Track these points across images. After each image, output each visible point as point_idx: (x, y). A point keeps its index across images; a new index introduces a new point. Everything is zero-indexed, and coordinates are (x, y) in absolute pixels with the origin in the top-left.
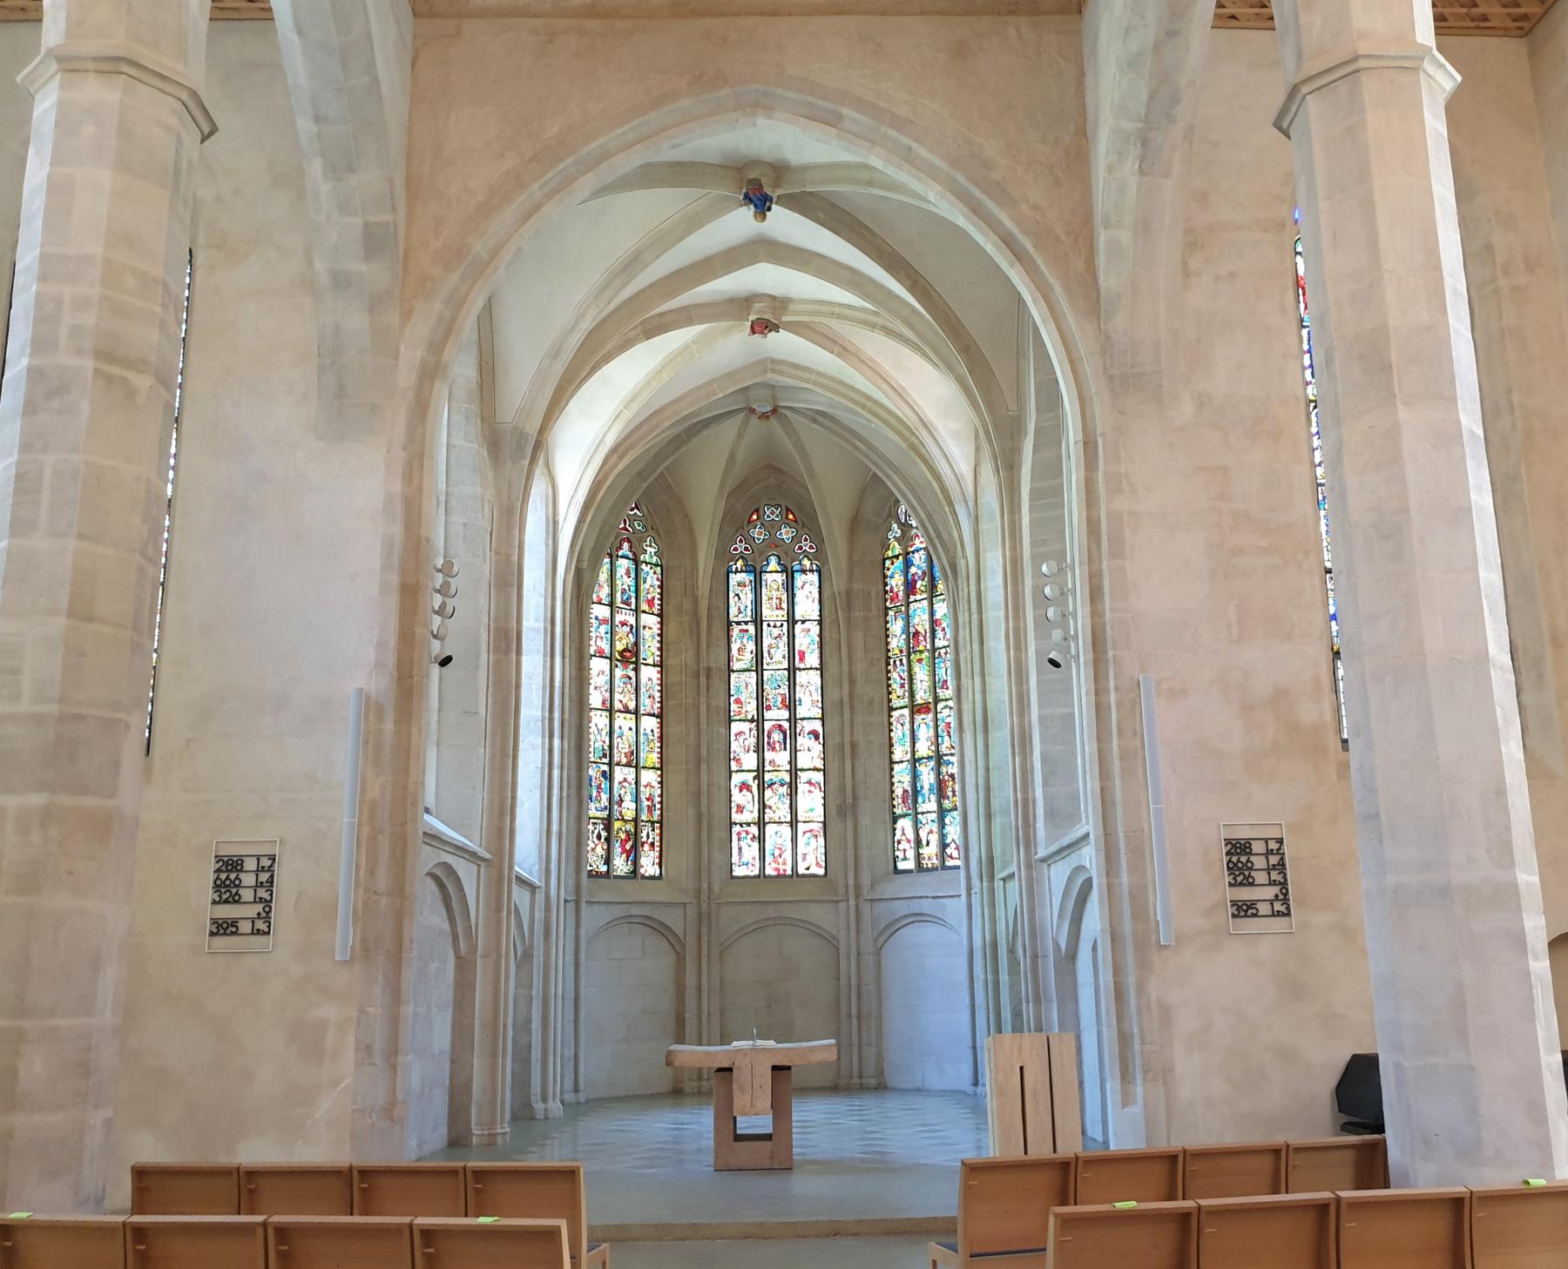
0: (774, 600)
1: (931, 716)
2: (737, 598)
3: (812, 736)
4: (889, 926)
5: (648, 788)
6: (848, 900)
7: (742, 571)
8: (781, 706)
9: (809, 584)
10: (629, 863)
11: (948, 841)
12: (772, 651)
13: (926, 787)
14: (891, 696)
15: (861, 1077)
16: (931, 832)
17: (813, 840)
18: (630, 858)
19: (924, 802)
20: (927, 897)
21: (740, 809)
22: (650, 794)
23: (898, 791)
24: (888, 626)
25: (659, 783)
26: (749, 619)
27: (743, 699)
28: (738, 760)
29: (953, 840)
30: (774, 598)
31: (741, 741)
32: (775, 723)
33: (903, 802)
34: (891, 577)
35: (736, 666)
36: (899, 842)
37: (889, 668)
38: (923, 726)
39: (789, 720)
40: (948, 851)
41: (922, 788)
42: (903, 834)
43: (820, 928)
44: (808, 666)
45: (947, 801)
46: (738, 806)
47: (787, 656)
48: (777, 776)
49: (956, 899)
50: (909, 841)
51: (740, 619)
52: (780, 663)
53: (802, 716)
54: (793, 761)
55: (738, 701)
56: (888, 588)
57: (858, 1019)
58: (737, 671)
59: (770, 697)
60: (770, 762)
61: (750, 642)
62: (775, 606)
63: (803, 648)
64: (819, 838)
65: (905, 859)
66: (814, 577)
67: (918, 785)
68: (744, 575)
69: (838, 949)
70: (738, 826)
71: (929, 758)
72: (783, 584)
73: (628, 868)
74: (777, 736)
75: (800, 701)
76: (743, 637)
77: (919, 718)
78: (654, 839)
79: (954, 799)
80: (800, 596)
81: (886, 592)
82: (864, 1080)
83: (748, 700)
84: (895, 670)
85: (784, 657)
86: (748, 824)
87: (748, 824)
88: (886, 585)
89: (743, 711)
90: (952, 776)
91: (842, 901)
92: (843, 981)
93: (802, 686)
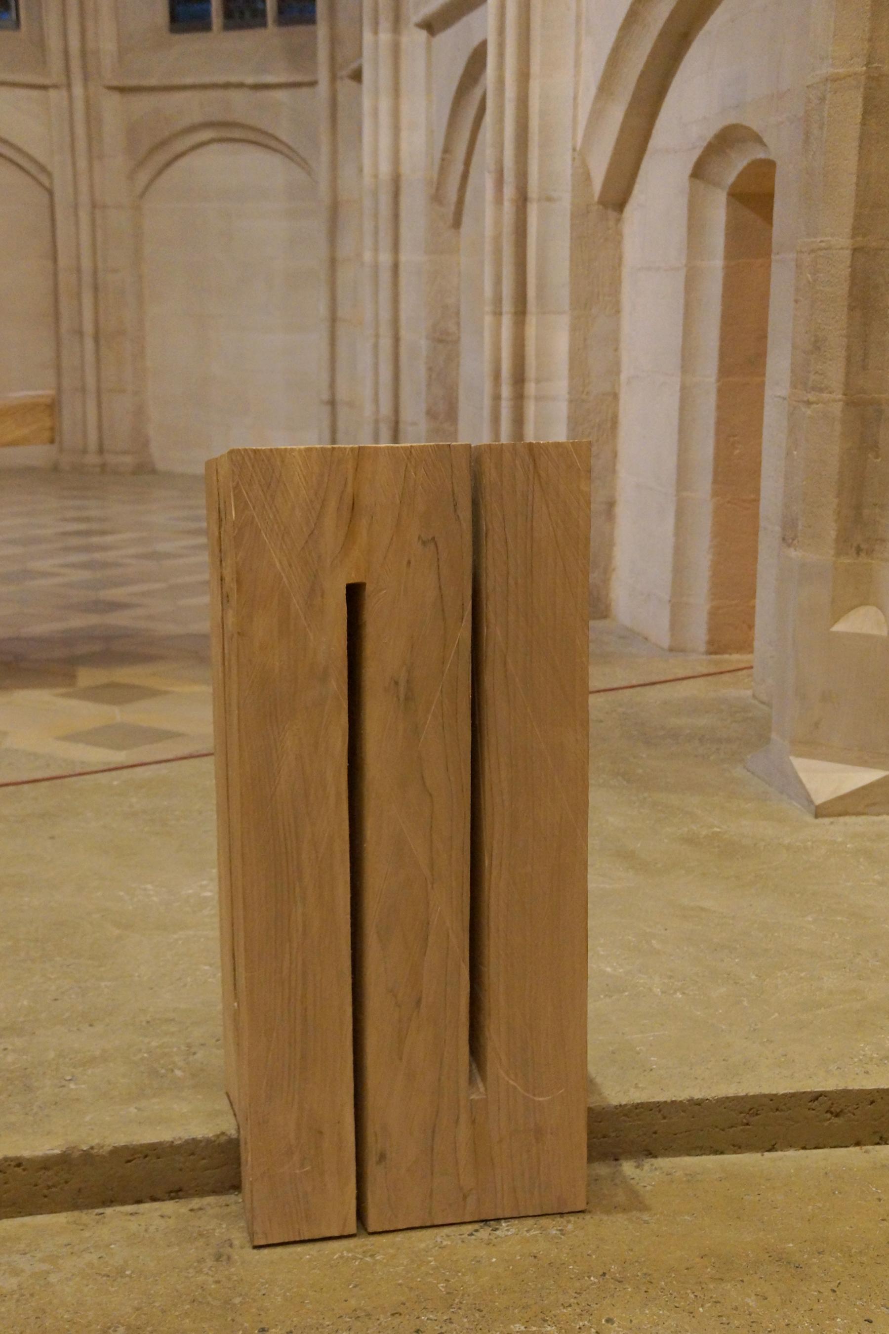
4: (164, 143)
6: (69, 86)
15: (101, 451)
20: (240, 86)
43: (19, 150)
49: (305, 91)
57: (96, 339)
69: (51, 193)
82: (111, 459)
91: (55, 86)
92: (63, 261)
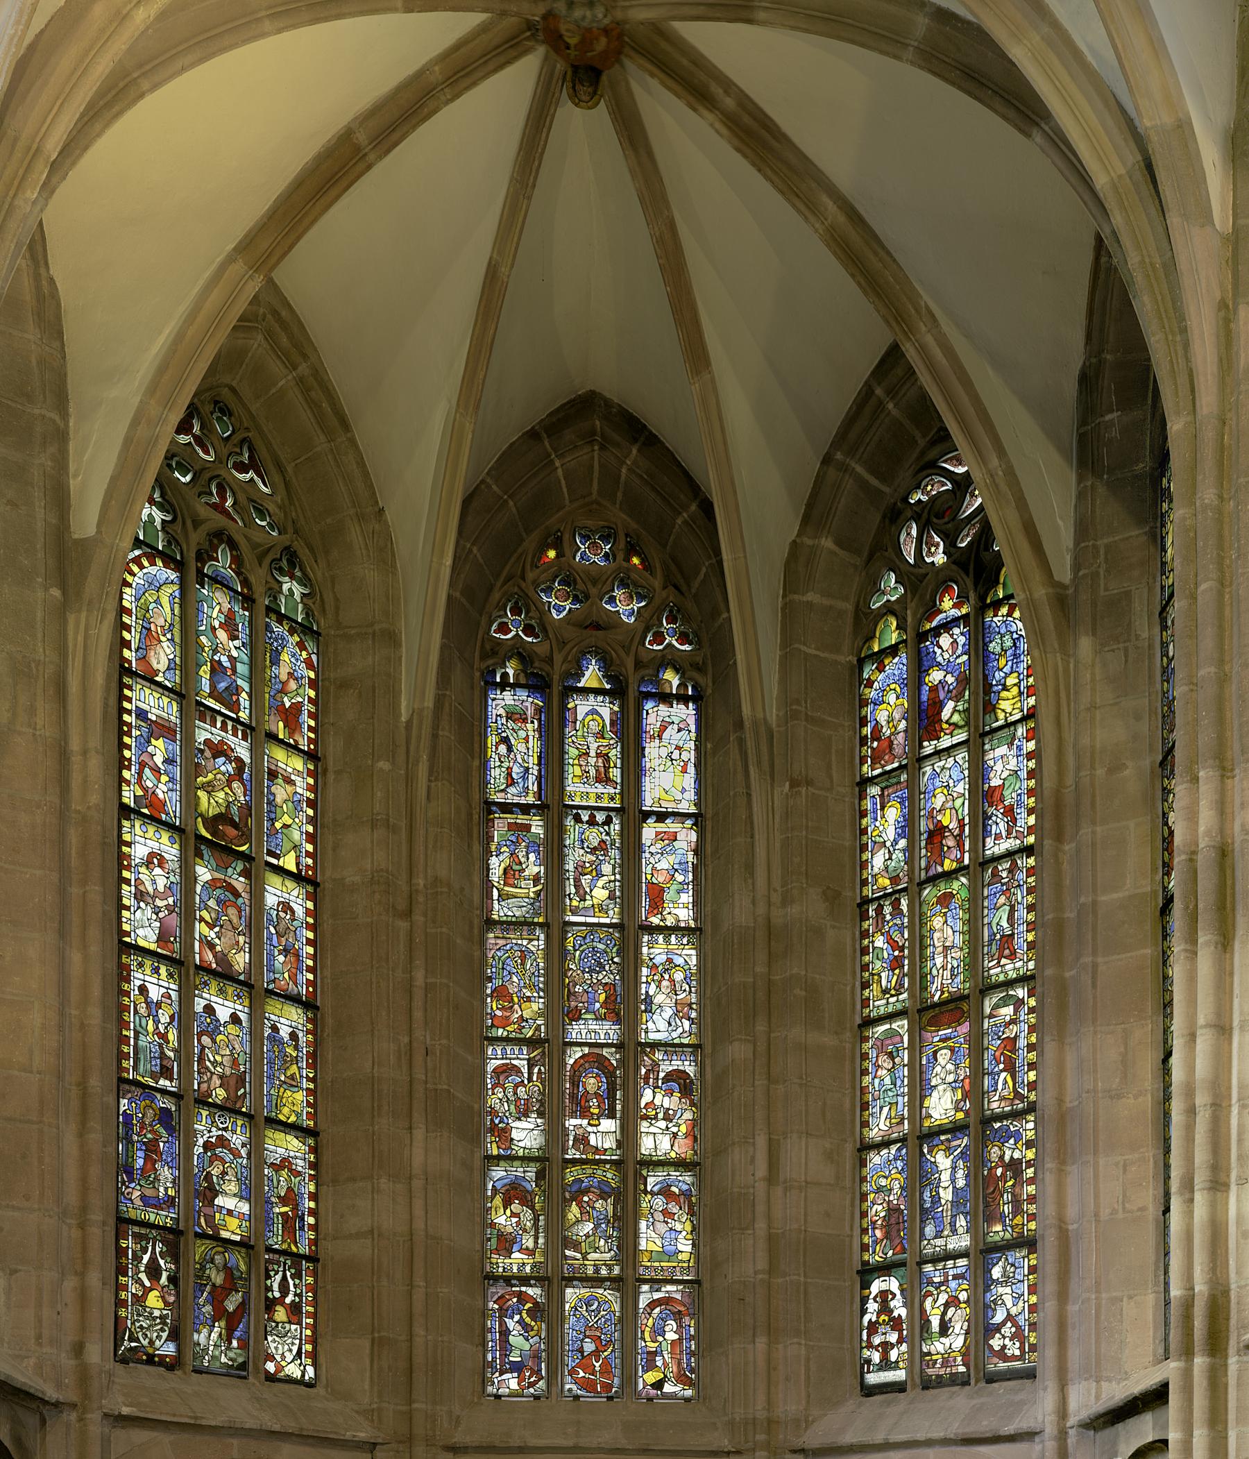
0: (592, 761)
1: (965, 1028)
2: (503, 749)
5: (284, 1173)
7: (514, 686)
9: (676, 727)
10: (235, 1343)
11: (1000, 1317)
12: (586, 880)
13: (946, 1195)
14: (866, 993)
16: (953, 1302)
17: (672, 1324)
18: (237, 1334)
19: (938, 1235)
21: (506, 1244)
22: (290, 1189)
23: (878, 1210)
24: (864, 821)
25: (313, 1166)
26: (531, 799)
27: (512, 989)
28: (504, 1134)
29: (1009, 1317)
30: (593, 753)
32: (586, 1050)
33: (887, 1236)
34: (876, 703)
35: (500, 911)
36: (873, 1328)
37: (865, 925)
38: (944, 1056)
39: (619, 1046)
40: (996, 1343)
41: (936, 1199)
42: (885, 1308)
44: (670, 921)
45: (998, 1228)
46: (501, 1236)
47: (618, 893)
48: (592, 1176)
50: (896, 1324)
51: (513, 795)
52: (602, 909)
53: (653, 1036)
54: (628, 1137)
55: (501, 993)
56: (867, 730)
58: (501, 923)
61: (532, 857)
62: (593, 772)
63: (660, 878)
65: (886, 1365)
66: (685, 713)
67: (927, 1196)
68: (523, 694)
70: (501, 1283)
71: (956, 1129)
72: (613, 723)
73: (231, 1354)
74: (591, 1083)
75: (649, 1000)
76: (516, 843)
77: (934, 1037)
78: (300, 1295)
79: (1018, 1220)
80: (653, 751)
81: (863, 741)
83: (528, 994)
84: (879, 930)
85: (611, 897)
86: (525, 1280)
87: (525, 1280)
88: (863, 722)
90: (1015, 1167)
93: (655, 967)
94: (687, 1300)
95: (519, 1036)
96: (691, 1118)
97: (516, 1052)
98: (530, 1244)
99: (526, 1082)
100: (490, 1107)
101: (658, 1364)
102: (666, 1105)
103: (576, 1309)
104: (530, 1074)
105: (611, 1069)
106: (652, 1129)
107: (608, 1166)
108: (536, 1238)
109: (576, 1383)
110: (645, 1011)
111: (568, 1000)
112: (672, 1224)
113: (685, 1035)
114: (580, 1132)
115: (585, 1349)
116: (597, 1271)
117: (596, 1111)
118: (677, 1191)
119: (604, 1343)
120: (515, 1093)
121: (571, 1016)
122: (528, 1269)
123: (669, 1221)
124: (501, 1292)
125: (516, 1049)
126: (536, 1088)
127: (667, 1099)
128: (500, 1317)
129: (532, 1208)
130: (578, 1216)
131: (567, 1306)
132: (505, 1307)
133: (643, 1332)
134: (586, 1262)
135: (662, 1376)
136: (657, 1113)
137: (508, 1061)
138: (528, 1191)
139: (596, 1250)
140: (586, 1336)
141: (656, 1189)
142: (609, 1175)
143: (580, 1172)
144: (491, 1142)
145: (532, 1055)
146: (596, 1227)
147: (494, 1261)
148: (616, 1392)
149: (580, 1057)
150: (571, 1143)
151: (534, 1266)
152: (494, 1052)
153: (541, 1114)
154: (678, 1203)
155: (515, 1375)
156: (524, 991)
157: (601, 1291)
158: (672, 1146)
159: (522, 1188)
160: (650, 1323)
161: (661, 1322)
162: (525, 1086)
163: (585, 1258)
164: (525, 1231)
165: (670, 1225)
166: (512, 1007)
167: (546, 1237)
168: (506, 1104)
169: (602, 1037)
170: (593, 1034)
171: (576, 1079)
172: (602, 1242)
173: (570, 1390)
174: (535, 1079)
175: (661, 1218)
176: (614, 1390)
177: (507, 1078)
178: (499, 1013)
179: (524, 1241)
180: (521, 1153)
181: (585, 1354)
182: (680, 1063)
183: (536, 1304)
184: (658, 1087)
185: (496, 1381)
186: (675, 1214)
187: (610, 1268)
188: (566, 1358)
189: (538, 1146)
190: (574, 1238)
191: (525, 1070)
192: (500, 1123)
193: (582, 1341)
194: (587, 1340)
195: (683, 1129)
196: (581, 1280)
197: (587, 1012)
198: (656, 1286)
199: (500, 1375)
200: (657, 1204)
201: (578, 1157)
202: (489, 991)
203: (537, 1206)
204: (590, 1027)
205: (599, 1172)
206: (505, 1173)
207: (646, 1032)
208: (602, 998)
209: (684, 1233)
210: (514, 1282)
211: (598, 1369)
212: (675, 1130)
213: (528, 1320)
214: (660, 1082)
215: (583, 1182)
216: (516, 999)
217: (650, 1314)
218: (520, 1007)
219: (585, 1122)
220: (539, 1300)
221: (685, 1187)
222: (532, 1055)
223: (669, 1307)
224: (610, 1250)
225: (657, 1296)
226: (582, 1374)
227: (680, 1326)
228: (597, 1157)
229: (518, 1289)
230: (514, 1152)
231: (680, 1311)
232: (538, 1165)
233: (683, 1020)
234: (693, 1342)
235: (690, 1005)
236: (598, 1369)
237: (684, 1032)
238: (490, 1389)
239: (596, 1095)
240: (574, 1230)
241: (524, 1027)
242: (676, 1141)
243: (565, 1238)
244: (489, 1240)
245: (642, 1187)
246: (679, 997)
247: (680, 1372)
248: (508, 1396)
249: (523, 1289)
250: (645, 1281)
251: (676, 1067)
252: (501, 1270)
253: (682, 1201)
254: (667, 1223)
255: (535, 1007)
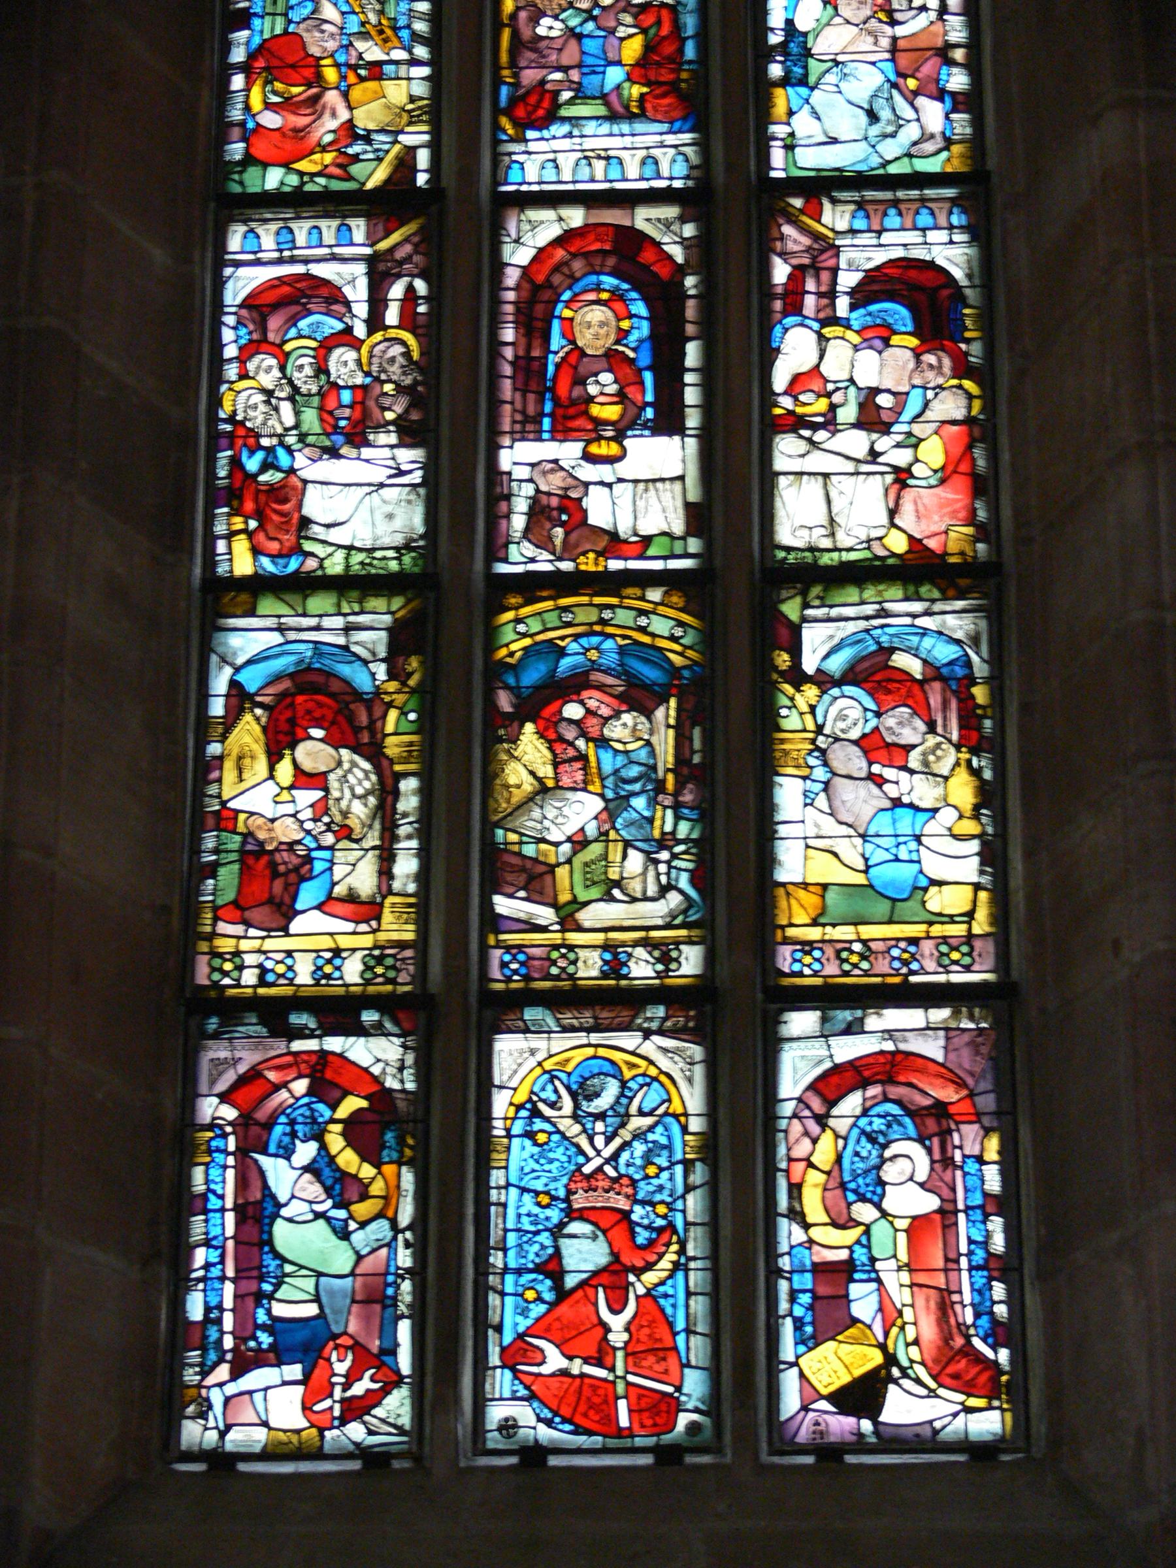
3: (899, 314)
8: (636, 91)
31: (301, 349)
32: (576, 217)
53: (811, 159)
59: (547, 27)
60: (538, 511)
64: (968, 1138)
70: (253, 1027)
83: (373, 52)
89: (326, 128)
94: (965, 1060)
95: (336, 185)
96: (960, 414)
97: (329, 237)
98: (364, 880)
99: (360, 330)
100: (231, 419)
101: (857, 1310)
102: (867, 379)
103: (536, 1113)
104: (377, 303)
105: (663, 271)
106: (818, 462)
107: (655, 595)
108: (386, 858)
109: (531, 1397)
110: (785, 82)
111: (513, 64)
112: (902, 784)
113: (929, 147)
114: (553, 483)
115: (569, 1262)
116: (615, 967)
117: (612, 412)
118: (915, 667)
119: (642, 1237)
120: (321, 369)
121: (521, 112)
122: (352, 971)
123: (889, 773)
124: (248, 1058)
125: (329, 228)
126: (397, 350)
127: (868, 357)
128: (242, 1153)
129: (374, 752)
130: (546, 771)
131: (500, 1104)
132: (261, 1115)
133: (796, 1190)
134: (574, 938)
135: (876, 1358)
136: (833, 408)
137: (299, 269)
138: (357, 695)
139: (610, 888)
140: (572, 1214)
141: (836, 664)
142: (660, 626)
143: (552, 619)
144: (230, 536)
145: (384, 245)
146: (614, 807)
147: (225, 945)
148: (693, 1428)
149: (558, 242)
150: (518, 522)
151: (376, 957)
152: (251, 244)
153: (408, 434)
154: (922, 710)
155: (295, 1371)
156: (360, 45)
157: (629, 1040)
158: (892, 513)
159: (335, 686)
160: (824, 1154)
161: (866, 1147)
162: (356, 344)
163: (568, 922)
164: (345, 833)
165: (892, 790)
166: (316, 99)
167: (424, 854)
168: (286, 408)
169: (633, 171)
170: (599, 165)
171: (539, 309)
172: (635, 861)
173: (508, 1427)
174: (392, 316)
175: (856, 763)
176: (683, 1420)
177: (293, 321)
178: (271, 120)
179: (339, 872)
180: (335, 566)
181: (570, 1281)
182: (912, 237)
183: (380, 1097)
184: (834, 321)
185: (217, 1397)
186: (909, 748)
187: (665, 955)
188: (493, 1299)
189: (399, 540)
190: (529, 850)
191: (358, 293)
192: (265, 467)
193: (557, 1232)
194: (575, 1227)
195: (933, 453)
196: (556, 1001)
197: (581, 96)
198: (845, 1016)
199: (235, 1375)
200: (841, 717)
201: (548, 567)
202: (238, 55)
203: (393, 746)
204: (589, 144)
205: (624, 617)
206: (276, 638)
207: (790, 148)
208: (633, 49)
209: (947, 816)
210: (299, 1019)
211: (618, 1338)
212: (902, 458)
213: (348, 1160)
214: (842, 306)
215: (562, 652)
216: (331, 74)
217: (822, 1120)
218: (345, 95)
219: (569, 451)
220: (391, 1083)
221: (944, 653)
222: (384, 245)
223: (895, 1091)
224: (664, 890)
225: (848, 1049)
226: (555, 1361)
227: (944, 1162)
228: (615, 565)
229: (312, 1045)
230: (311, 564)
231: (940, 1109)
232: (397, 602)
233: (921, 101)
234: (996, 1224)
235: (943, 53)
236: (618, 1338)
237: (926, 137)
238: (193, 1433)
239: (613, 360)
240: (530, 823)
241: (356, 159)
242: (908, 496)
243: (493, 853)
244: (212, 870)
245: (783, 660)
246: (900, 31)
247: (947, 1338)
248: (266, 1455)
249: (334, 1044)
250: (803, 998)
251: (899, 253)
252: (249, 977)
253: (935, 700)
254: (879, 781)
255: (396, 93)
